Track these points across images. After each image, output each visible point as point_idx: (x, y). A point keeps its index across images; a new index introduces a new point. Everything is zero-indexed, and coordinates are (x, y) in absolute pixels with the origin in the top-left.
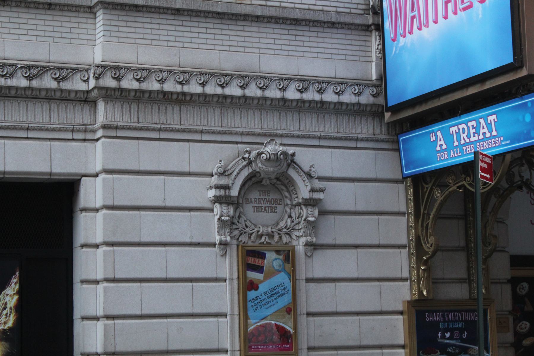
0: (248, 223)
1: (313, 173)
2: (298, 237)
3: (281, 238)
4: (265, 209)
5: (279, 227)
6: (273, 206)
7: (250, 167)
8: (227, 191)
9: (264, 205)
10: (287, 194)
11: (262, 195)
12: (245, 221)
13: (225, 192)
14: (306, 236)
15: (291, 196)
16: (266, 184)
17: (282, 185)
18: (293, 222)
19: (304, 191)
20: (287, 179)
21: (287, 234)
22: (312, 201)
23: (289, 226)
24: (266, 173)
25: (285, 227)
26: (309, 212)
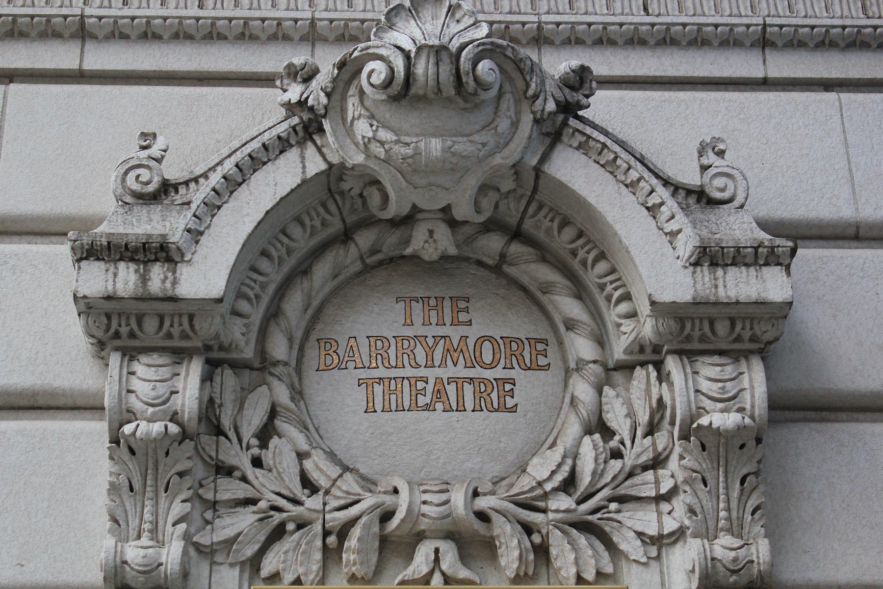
0: (320, 468)
1: (719, 182)
2: (660, 542)
3: (542, 552)
4: (439, 394)
5: (524, 483)
6: (489, 374)
7: (310, 150)
8: (157, 272)
9: (431, 374)
10: (572, 308)
11: (418, 319)
12: (301, 456)
13: (144, 279)
14: (708, 534)
15: (597, 315)
16: (430, 254)
17: (544, 260)
18: (617, 454)
19: (658, 265)
20: (565, 223)
21: (584, 527)
22: (722, 328)
23: (585, 480)
24: (413, 169)
25: (569, 484)
26: (705, 386)
